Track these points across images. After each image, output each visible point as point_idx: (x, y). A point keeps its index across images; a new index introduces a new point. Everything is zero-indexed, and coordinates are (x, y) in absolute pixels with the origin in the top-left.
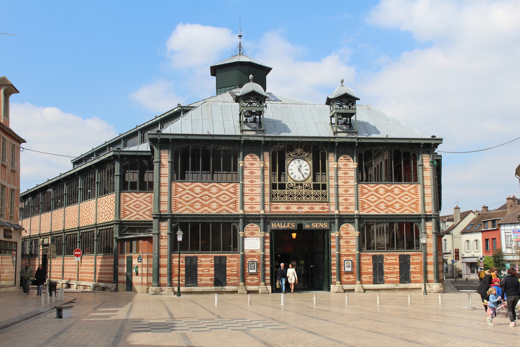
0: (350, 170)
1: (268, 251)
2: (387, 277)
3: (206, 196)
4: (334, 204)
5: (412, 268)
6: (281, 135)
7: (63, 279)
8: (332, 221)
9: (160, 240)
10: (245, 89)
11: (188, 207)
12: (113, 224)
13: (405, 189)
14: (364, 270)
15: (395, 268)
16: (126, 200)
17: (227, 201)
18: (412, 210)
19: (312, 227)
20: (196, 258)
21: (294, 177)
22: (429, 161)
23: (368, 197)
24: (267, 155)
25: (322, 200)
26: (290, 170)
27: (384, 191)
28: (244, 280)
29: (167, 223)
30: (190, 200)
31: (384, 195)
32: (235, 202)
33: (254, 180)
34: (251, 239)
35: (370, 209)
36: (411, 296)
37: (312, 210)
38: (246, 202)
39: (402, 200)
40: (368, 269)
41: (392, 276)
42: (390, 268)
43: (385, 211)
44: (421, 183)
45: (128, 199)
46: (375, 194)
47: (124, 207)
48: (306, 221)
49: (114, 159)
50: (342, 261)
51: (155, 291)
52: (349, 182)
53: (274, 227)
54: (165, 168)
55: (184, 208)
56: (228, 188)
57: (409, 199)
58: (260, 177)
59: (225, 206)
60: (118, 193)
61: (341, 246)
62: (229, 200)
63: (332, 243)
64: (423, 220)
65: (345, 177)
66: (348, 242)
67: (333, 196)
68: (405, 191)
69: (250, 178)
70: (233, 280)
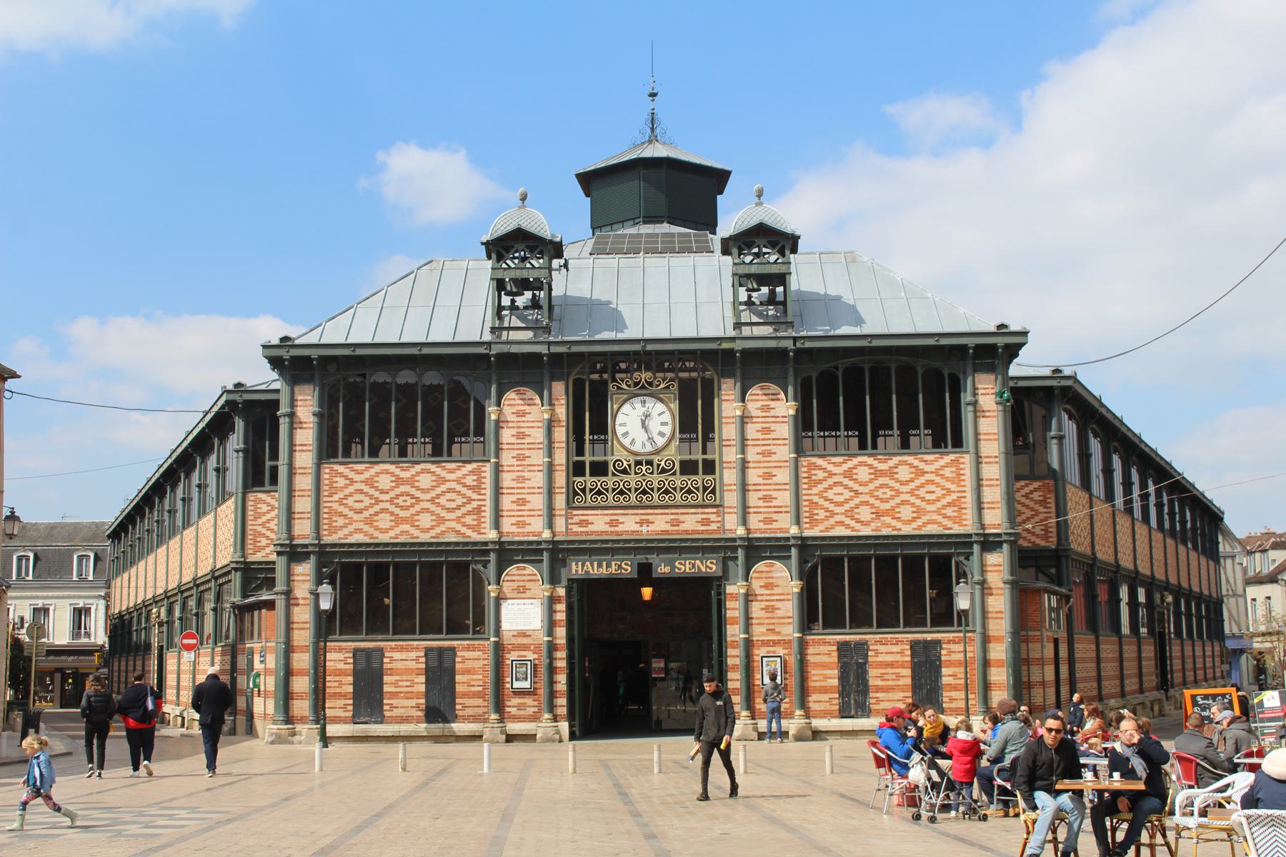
0: (779, 422)
1: (561, 632)
2: (878, 701)
3: (405, 498)
4: (735, 510)
5: (949, 676)
6: (598, 337)
7: (178, 705)
8: (729, 554)
9: (291, 607)
10: (500, 225)
11: (361, 525)
12: (229, 573)
13: (927, 468)
14: (815, 681)
15: (899, 676)
16: (259, 511)
17: (459, 508)
18: (945, 522)
19: (677, 570)
20: (381, 650)
21: (631, 444)
22: (993, 391)
23: (826, 490)
24: (559, 388)
25: (704, 500)
26: (620, 425)
27: (870, 474)
28: (499, 707)
29: (309, 566)
30: (366, 508)
31: (871, 485)
32: (478, 510)
33: (527, 453)
34: (518, 604)
35: (832, 521)
36: (831, 751)
37: (676, 528)
38: (507, 511)
39: (918, 497)
40: (826, 677)
41: (891, 695)
42: (886, 677)
43: (873, 525)
44: (972, 449)
45: (264, 508)
46: (845, 483)
47: (255, 527)
48: (661, 556)
49: (232, 410)
50: (756, 658)
51: (276, 735)
52: (775, 453)
53: (577, 571)
54: (305, 431)
55: (351, 528)
56: (460, 475)
57: (939, 492)
58: (541, 446)
59: (453, 520)
60: (240, 495)
61: (752, 618)
62: (464, 505)
63: (728, 612)
64: (976, 548)
65: (763, 440)
66: (774, 609)
67: (731, 490)
68: (927, 473)
69: (518, 449)
70: (473, 707)
